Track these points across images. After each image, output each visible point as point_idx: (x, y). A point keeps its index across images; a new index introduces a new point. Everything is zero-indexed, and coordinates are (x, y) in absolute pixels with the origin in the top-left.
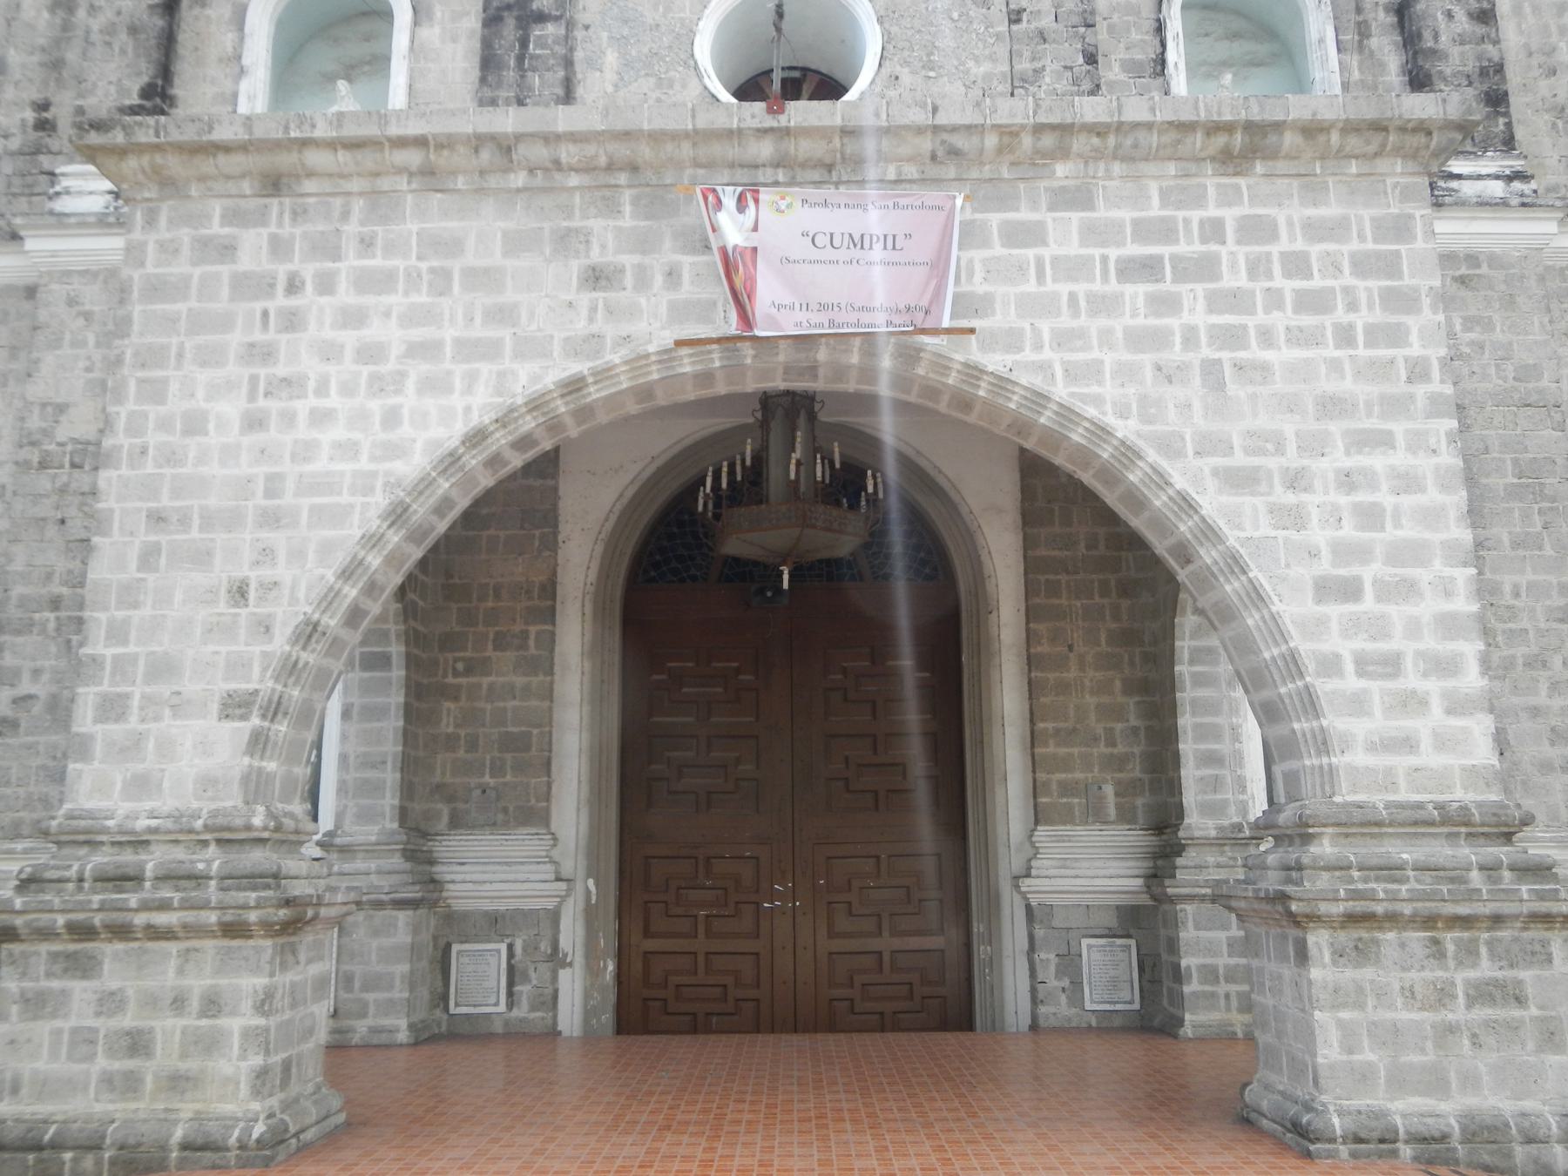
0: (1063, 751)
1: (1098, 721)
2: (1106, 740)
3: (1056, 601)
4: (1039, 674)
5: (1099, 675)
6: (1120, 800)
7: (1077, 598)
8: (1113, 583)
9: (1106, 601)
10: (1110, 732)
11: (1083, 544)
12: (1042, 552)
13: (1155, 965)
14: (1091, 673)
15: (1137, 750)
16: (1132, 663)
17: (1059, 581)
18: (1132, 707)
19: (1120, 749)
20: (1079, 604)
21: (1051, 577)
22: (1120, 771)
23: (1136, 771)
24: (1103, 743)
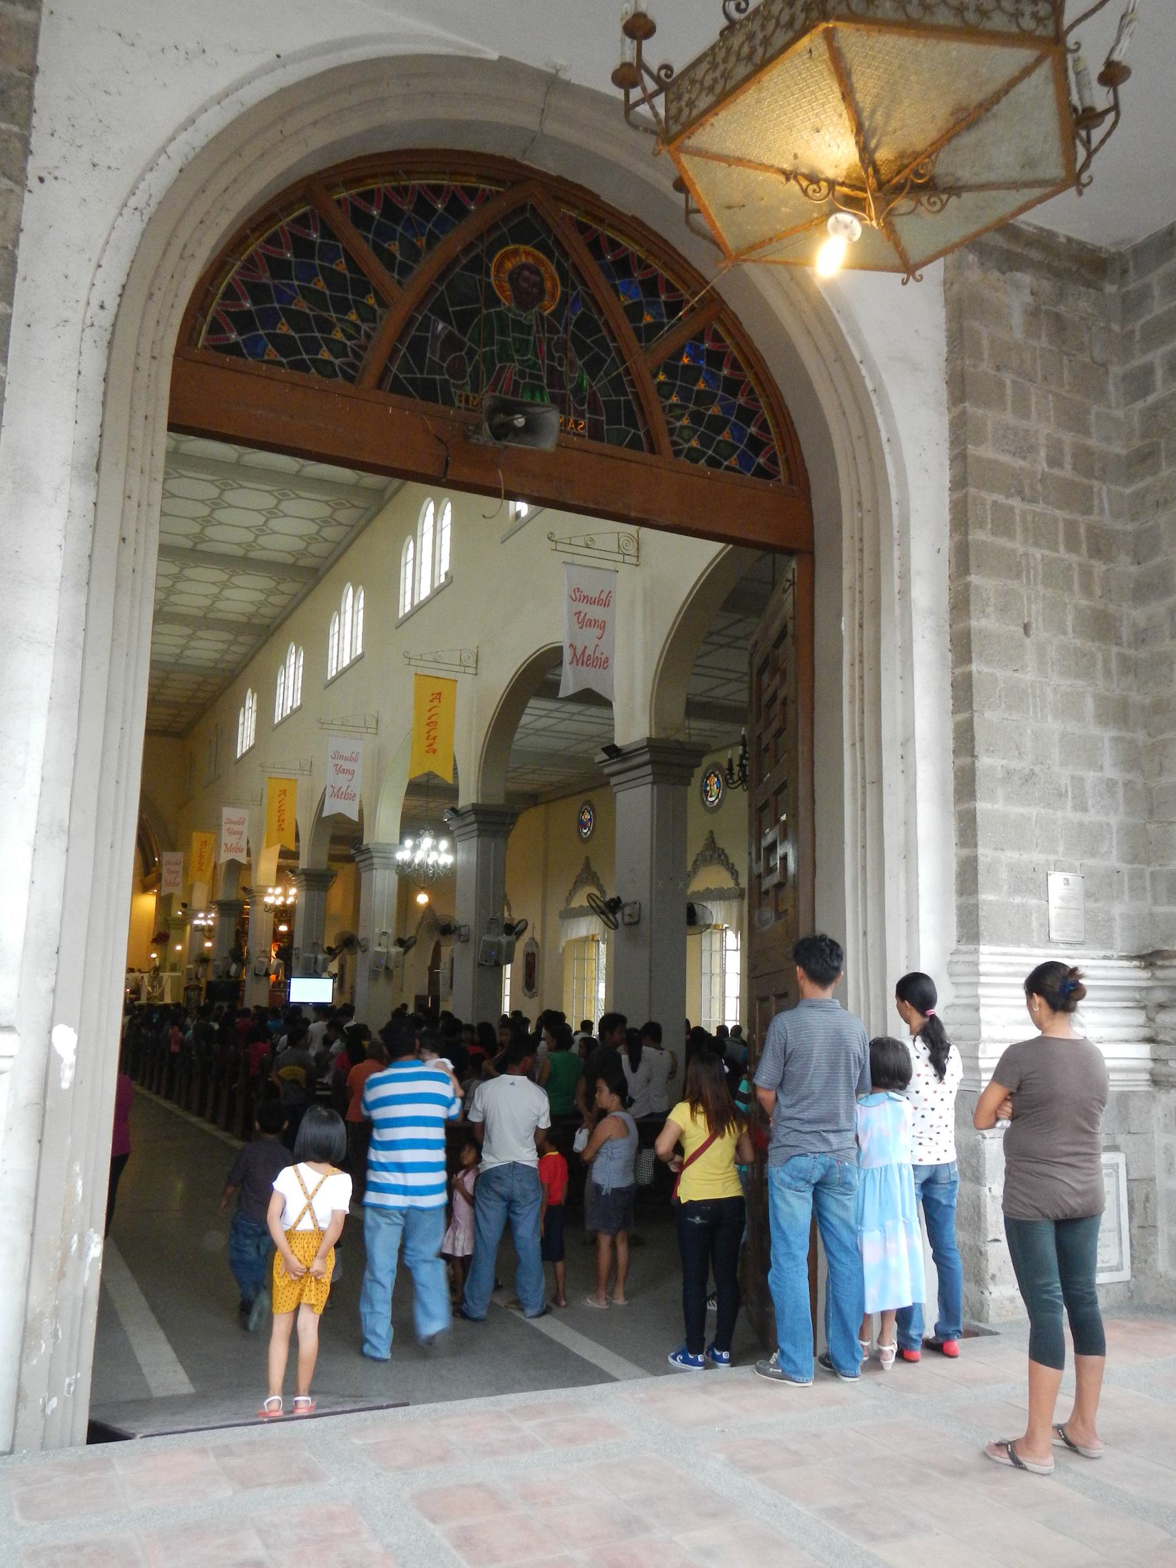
0: (1016, 810)
1: (1063, 764)
2: (1074, 798)
3: (1003, 542)
4: (986, 669)
5: (1065, 683)
6: (1092, 905)
7: (1036, 544)
8: (1082, 530)
9: (1074, 558)
10: (1078, 782)
11: (1043, 453)
12: (987, 452)
13: (1147, 1199)
14: (1055, 679)
15: (1114, 820)
16: (1107, 673)
17: (1012, 508)
18: (1107, 744)
19: (1093, 817)
20: (1039, 556)
21: (1001, 499)
22: (1093, 854)
23: (1111, 858)
24: (1070, 804)
